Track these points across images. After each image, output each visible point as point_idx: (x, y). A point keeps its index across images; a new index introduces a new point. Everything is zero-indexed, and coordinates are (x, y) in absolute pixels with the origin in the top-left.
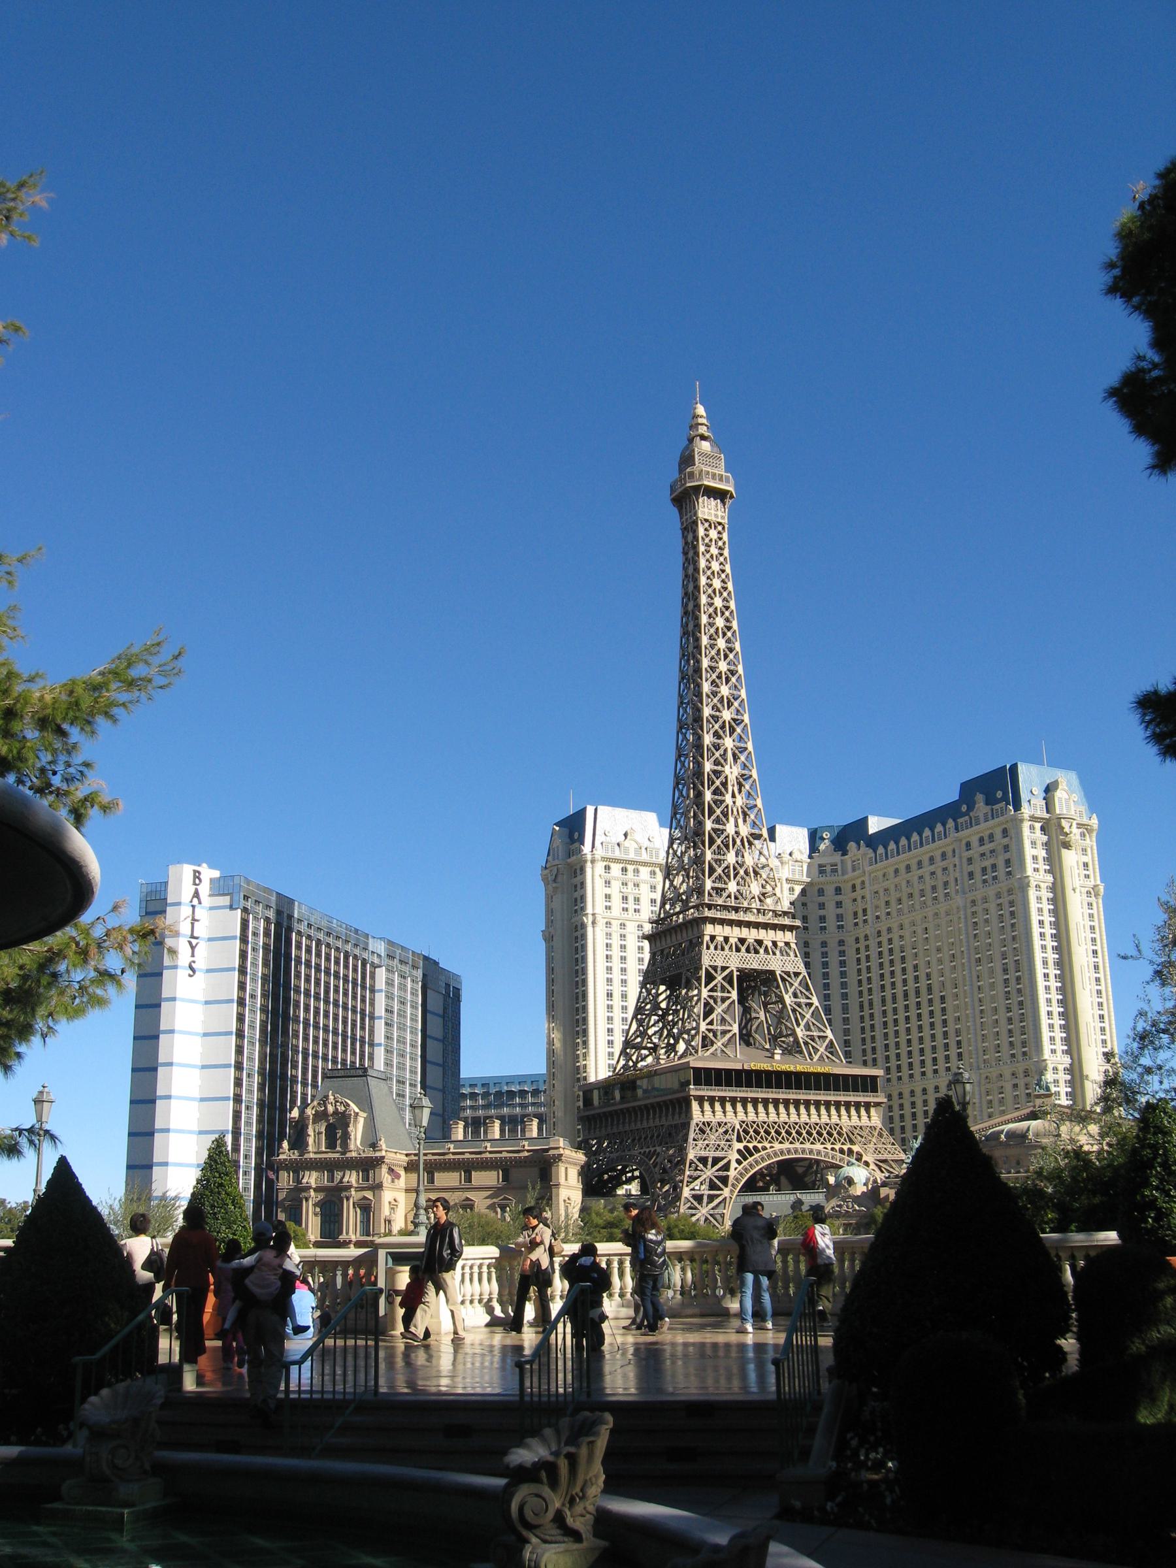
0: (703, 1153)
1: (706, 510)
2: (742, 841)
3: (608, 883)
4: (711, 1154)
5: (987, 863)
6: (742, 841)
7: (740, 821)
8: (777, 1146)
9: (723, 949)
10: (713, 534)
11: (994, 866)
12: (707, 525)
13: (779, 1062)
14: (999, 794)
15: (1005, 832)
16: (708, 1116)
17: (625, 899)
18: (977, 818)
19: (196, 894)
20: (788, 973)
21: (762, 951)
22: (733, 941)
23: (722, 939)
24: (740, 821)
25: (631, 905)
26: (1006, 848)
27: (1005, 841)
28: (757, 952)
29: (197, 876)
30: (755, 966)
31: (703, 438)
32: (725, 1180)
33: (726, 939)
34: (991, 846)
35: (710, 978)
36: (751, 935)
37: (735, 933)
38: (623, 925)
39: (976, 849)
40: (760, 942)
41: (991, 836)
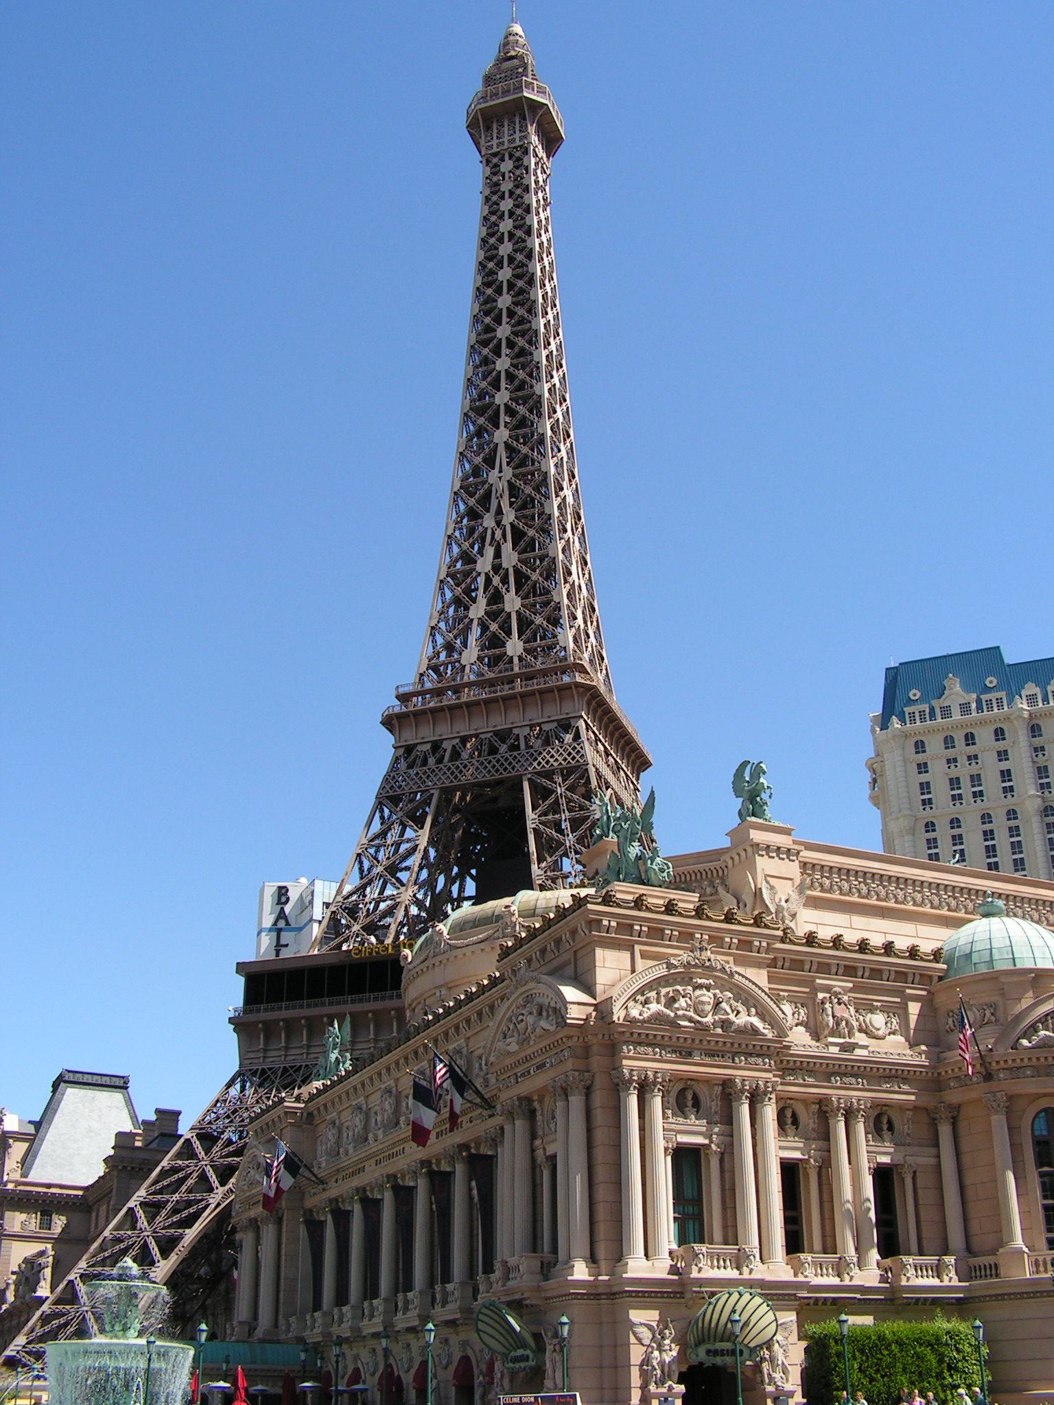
1: (495, 142)
2: (505, 581)
3: (923, 768)
6: (505, 581)
7: (507, 547)
9: (425, 763)
12: (495, 160)
17: (955, 783)
19: (281, 915)
20: (549, 775)
21: (503, 748)
22: (448, 746)
23: (428, 746)
24: (507, 547)
25: (966, 789)
28: (493, 751)
29: (282, 893)
33: (436, 746)
38: (955, 823)
40: (503, 735)
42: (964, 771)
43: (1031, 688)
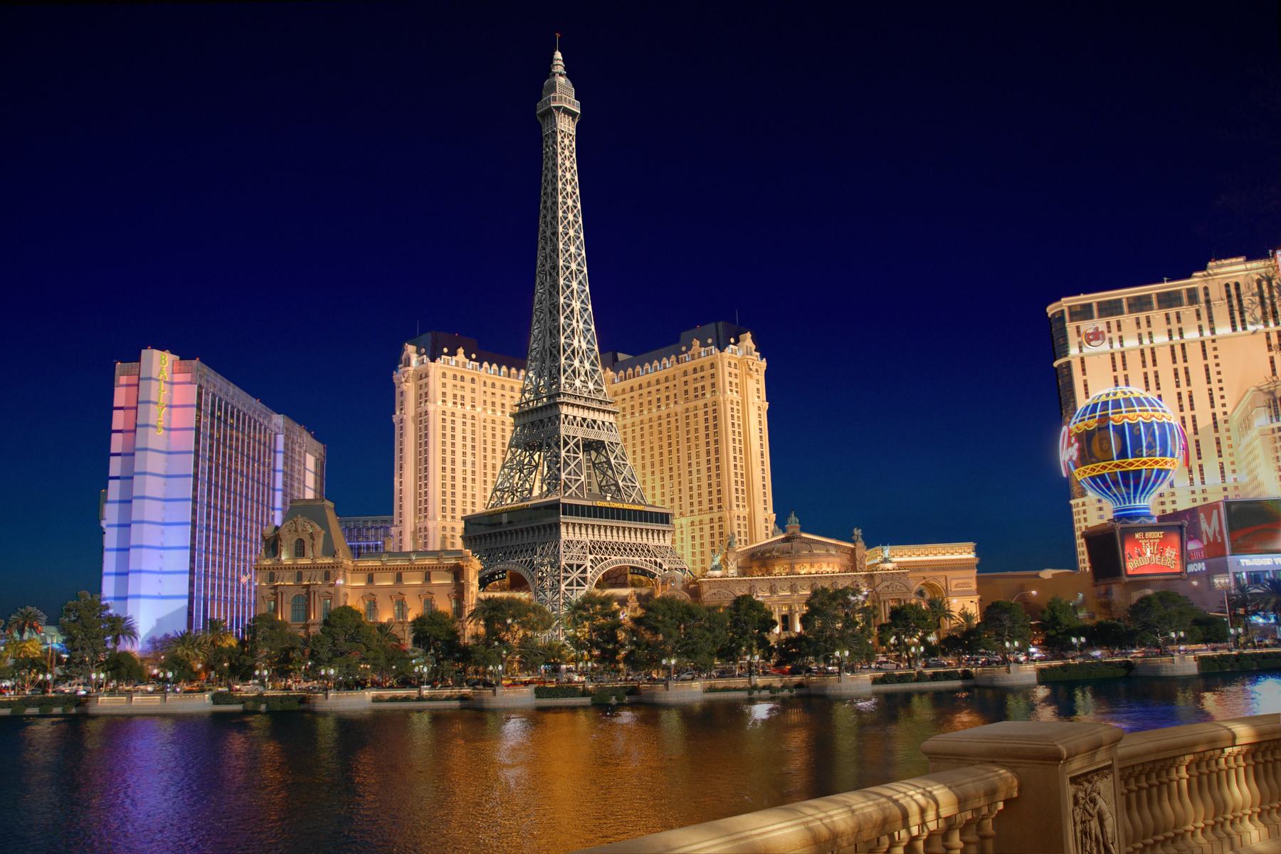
0: (571, 562)
4: (575, 562)
5: (699, 385)
8: (613, 558)
10: (567, 142)
11: (703, 387)
13: (608, 502)
14: (710, 341)
15: (712, 366)
16: (571, 537)
17: (455, 396)
18: (693, 355)
25: (459, 401)
26: (713, 376)
27: (712, 371)
30: (592, 437)
31: (561, 75)
32: (584, 579)
34: (702, 374)
35: (566, 444)
36: (590, 415)
37: (580, 414)
39: (689, 378)
40: (595, 421)
41: (702, 369)
42: (459, 393)
43: (486, 364)
